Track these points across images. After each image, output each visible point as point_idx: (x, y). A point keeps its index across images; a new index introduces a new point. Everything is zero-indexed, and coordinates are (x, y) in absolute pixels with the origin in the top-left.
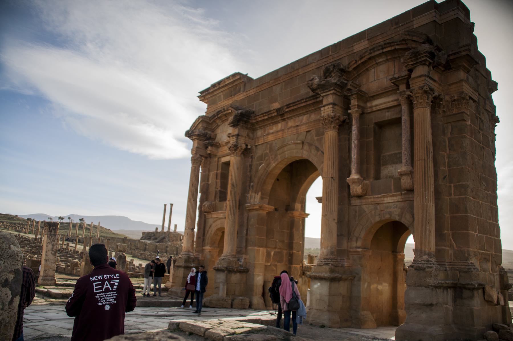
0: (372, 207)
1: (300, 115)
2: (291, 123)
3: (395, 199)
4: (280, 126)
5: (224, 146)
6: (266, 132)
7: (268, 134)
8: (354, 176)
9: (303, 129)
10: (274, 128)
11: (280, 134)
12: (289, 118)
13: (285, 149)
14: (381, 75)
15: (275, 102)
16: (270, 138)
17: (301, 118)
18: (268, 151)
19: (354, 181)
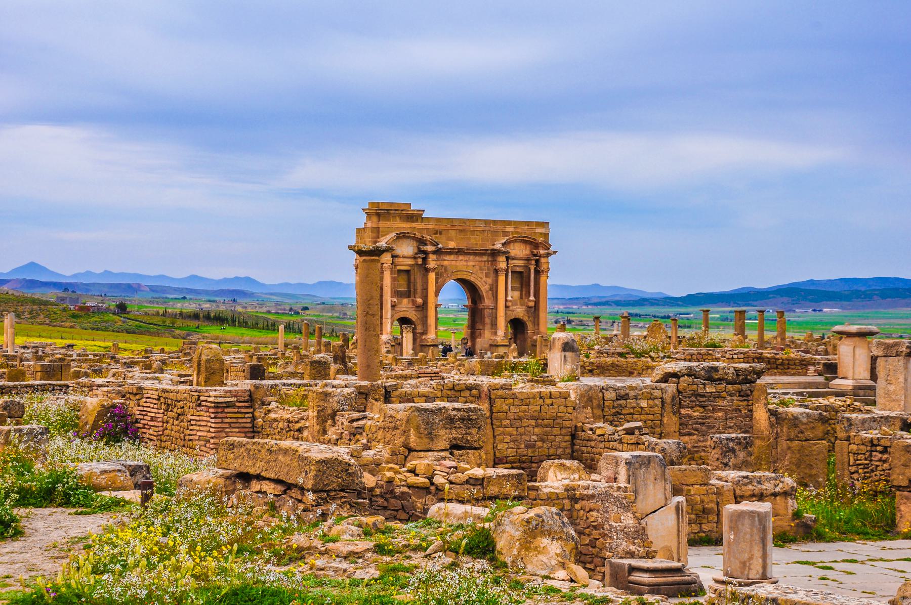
0: (511, 312)
1: (467, 255)
2: (461, 257)
3: (522, 309)
4: (452, 257)
5: (400, 257)
6: (441, 258)
7: (445, 260)
8: (509, 298)
9: (471, 263)
10: (447, 257)
11: (454, 263)
12: (461, 254)
13: (459, 273)
14: (517, 248)
15: (452, 241)
16: (446, 263)
17: (469, 256)
18: (443, 271)
19: (510, 301)
